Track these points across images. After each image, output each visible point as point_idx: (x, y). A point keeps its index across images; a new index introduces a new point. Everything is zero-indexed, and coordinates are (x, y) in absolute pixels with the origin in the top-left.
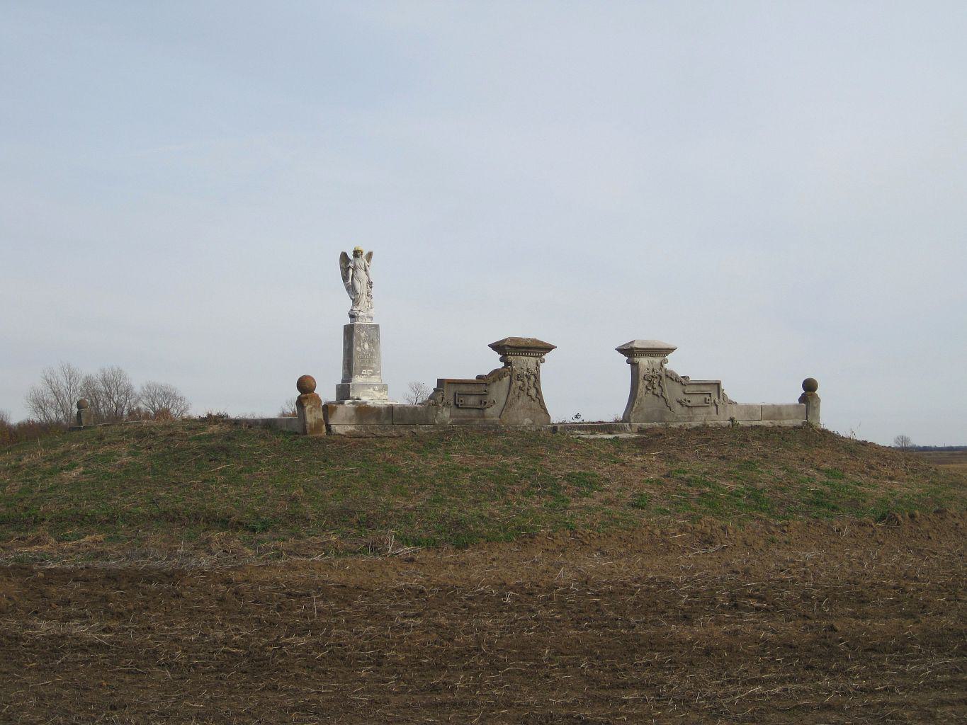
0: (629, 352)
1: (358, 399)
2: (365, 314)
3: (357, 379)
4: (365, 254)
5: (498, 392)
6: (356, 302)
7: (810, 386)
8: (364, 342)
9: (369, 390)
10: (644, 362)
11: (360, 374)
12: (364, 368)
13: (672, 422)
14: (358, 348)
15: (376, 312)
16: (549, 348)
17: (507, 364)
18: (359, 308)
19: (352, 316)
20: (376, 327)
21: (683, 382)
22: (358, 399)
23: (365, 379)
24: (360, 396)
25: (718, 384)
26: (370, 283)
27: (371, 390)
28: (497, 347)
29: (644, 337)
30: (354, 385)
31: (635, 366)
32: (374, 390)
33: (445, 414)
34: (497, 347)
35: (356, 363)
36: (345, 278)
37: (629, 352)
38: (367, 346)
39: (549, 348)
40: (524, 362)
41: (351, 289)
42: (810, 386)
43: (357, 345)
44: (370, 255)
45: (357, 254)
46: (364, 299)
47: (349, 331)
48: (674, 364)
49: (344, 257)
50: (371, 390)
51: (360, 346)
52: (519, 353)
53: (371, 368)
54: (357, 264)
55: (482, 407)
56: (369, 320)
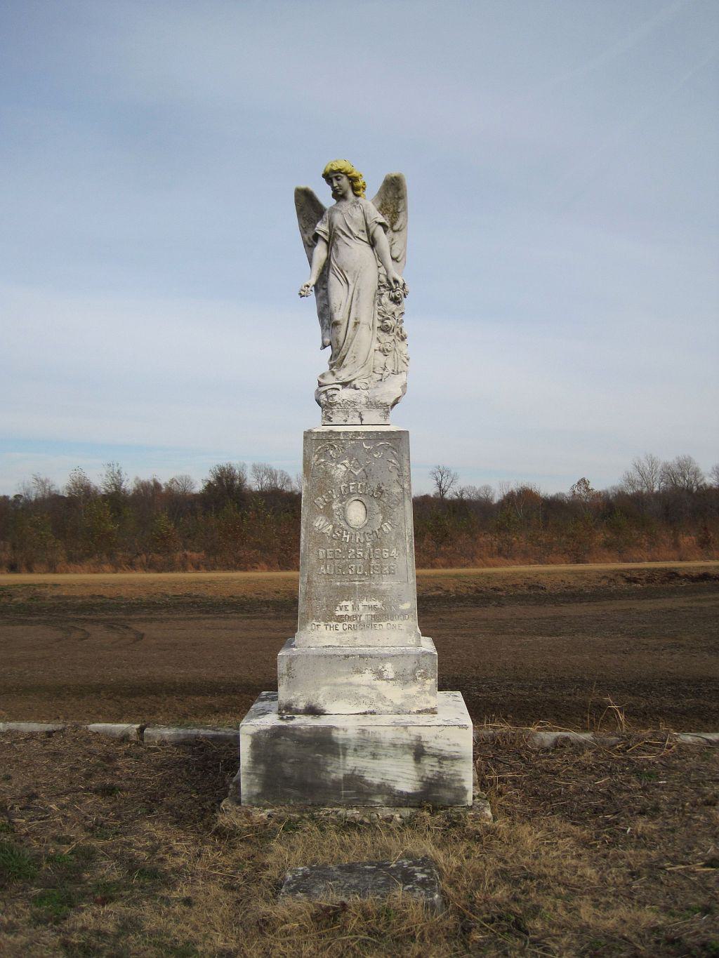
1: (313, 711)
2: (361, 396)
3: (316, 637)
4: (373, 185)
8: (345, 496)
9: (356, 679)
11: (330, 617)
12: (345, 593)
14: (320, 523)
18: (344, 375)
19: (327, 407)
20: (397, 441)
22: (313, 711)
23: (350, 634)
24: (321, 701)
26: (392, 290)
27: (368, 677)
30: (292, 659)
32: (380, 675)
38: (356, 513)
43: (315, 511)
44: (393, 189)
45: (343, 182)
46: (365, 341)
50: (368, 677)
51: (328, 512)
53: (376, 594)
54: (338, 218)
56: (373, 416)
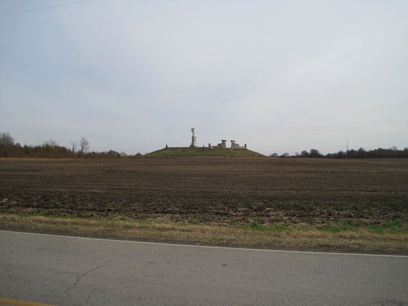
0: (232, 141)
3: (194, 143)
5: (222, 145)
6: (193, 134)
7: (246, 145)
10: (233, 142)
13: (235, 148)
15: (195, 135)
16: (226, 141)
17: (223, 142)
21: (236, 144)
25: (238, 144)
28: (222, 141)
29: (233, 140)
31: (232, 143)
33: (219, 147)
34: (222, 141)
35: (194, 141)
36: (192, 131)
37: (232, 141)
39: (226, 141)
40: (224, 142)
41: (193, 132)
42: (246, 145)
47: (193, 137)
48: (235, 142)
49: (192, 129)
52: (224, 141)
55: (221, 146)
